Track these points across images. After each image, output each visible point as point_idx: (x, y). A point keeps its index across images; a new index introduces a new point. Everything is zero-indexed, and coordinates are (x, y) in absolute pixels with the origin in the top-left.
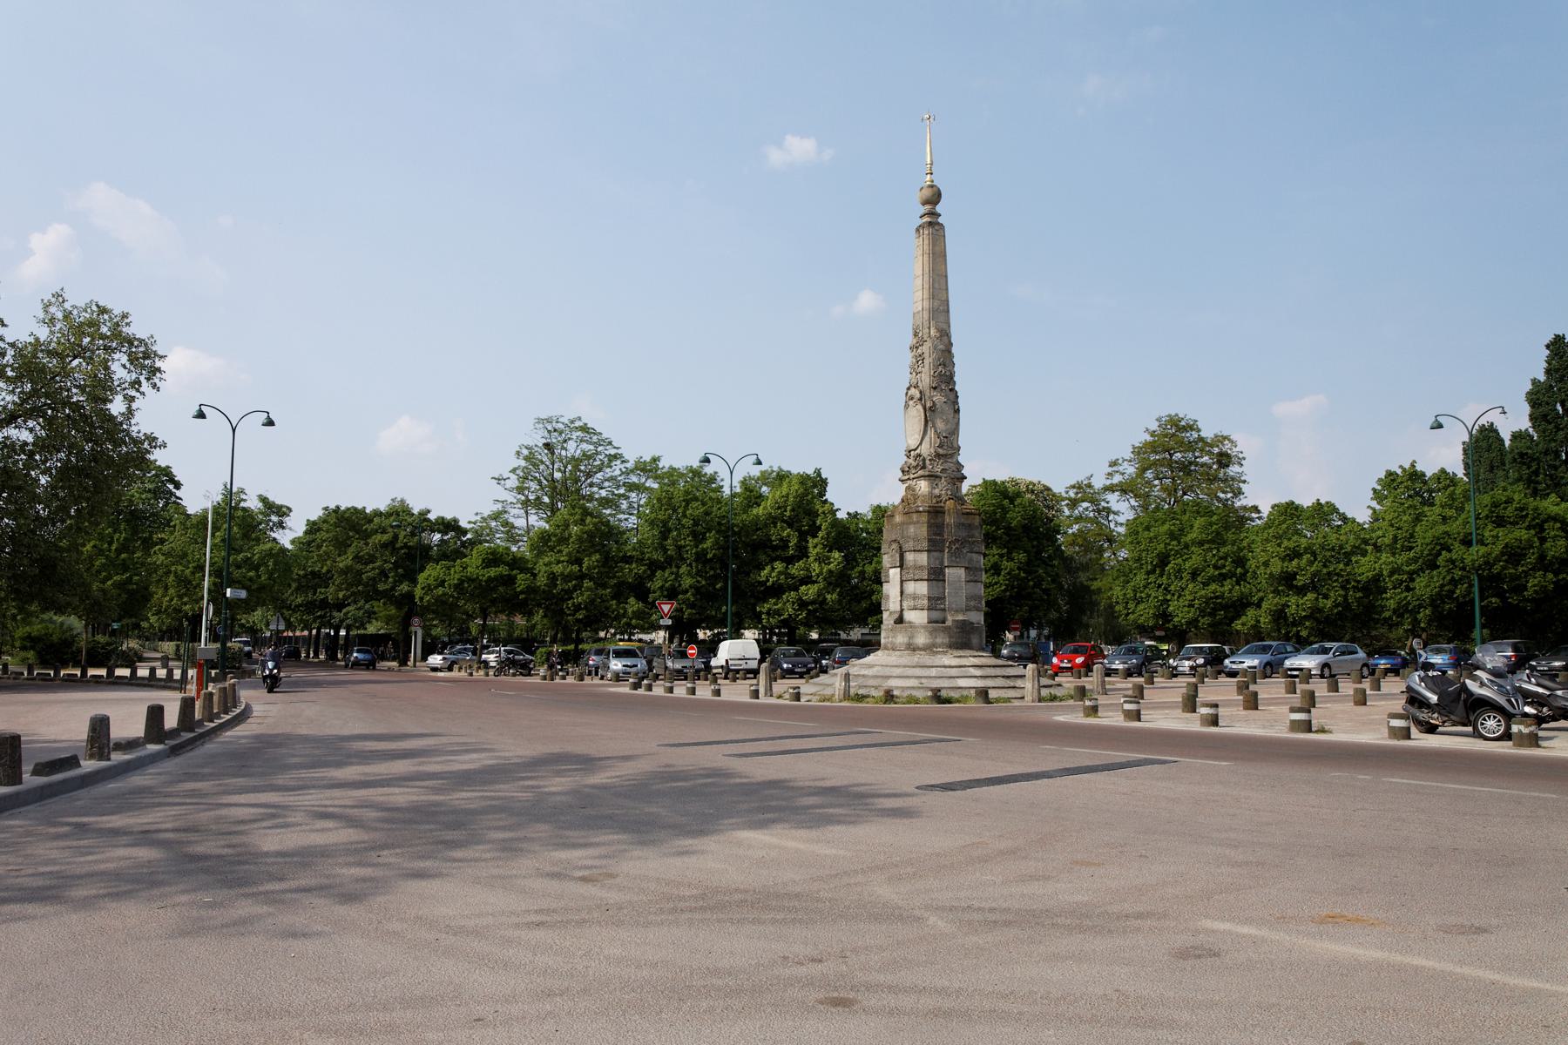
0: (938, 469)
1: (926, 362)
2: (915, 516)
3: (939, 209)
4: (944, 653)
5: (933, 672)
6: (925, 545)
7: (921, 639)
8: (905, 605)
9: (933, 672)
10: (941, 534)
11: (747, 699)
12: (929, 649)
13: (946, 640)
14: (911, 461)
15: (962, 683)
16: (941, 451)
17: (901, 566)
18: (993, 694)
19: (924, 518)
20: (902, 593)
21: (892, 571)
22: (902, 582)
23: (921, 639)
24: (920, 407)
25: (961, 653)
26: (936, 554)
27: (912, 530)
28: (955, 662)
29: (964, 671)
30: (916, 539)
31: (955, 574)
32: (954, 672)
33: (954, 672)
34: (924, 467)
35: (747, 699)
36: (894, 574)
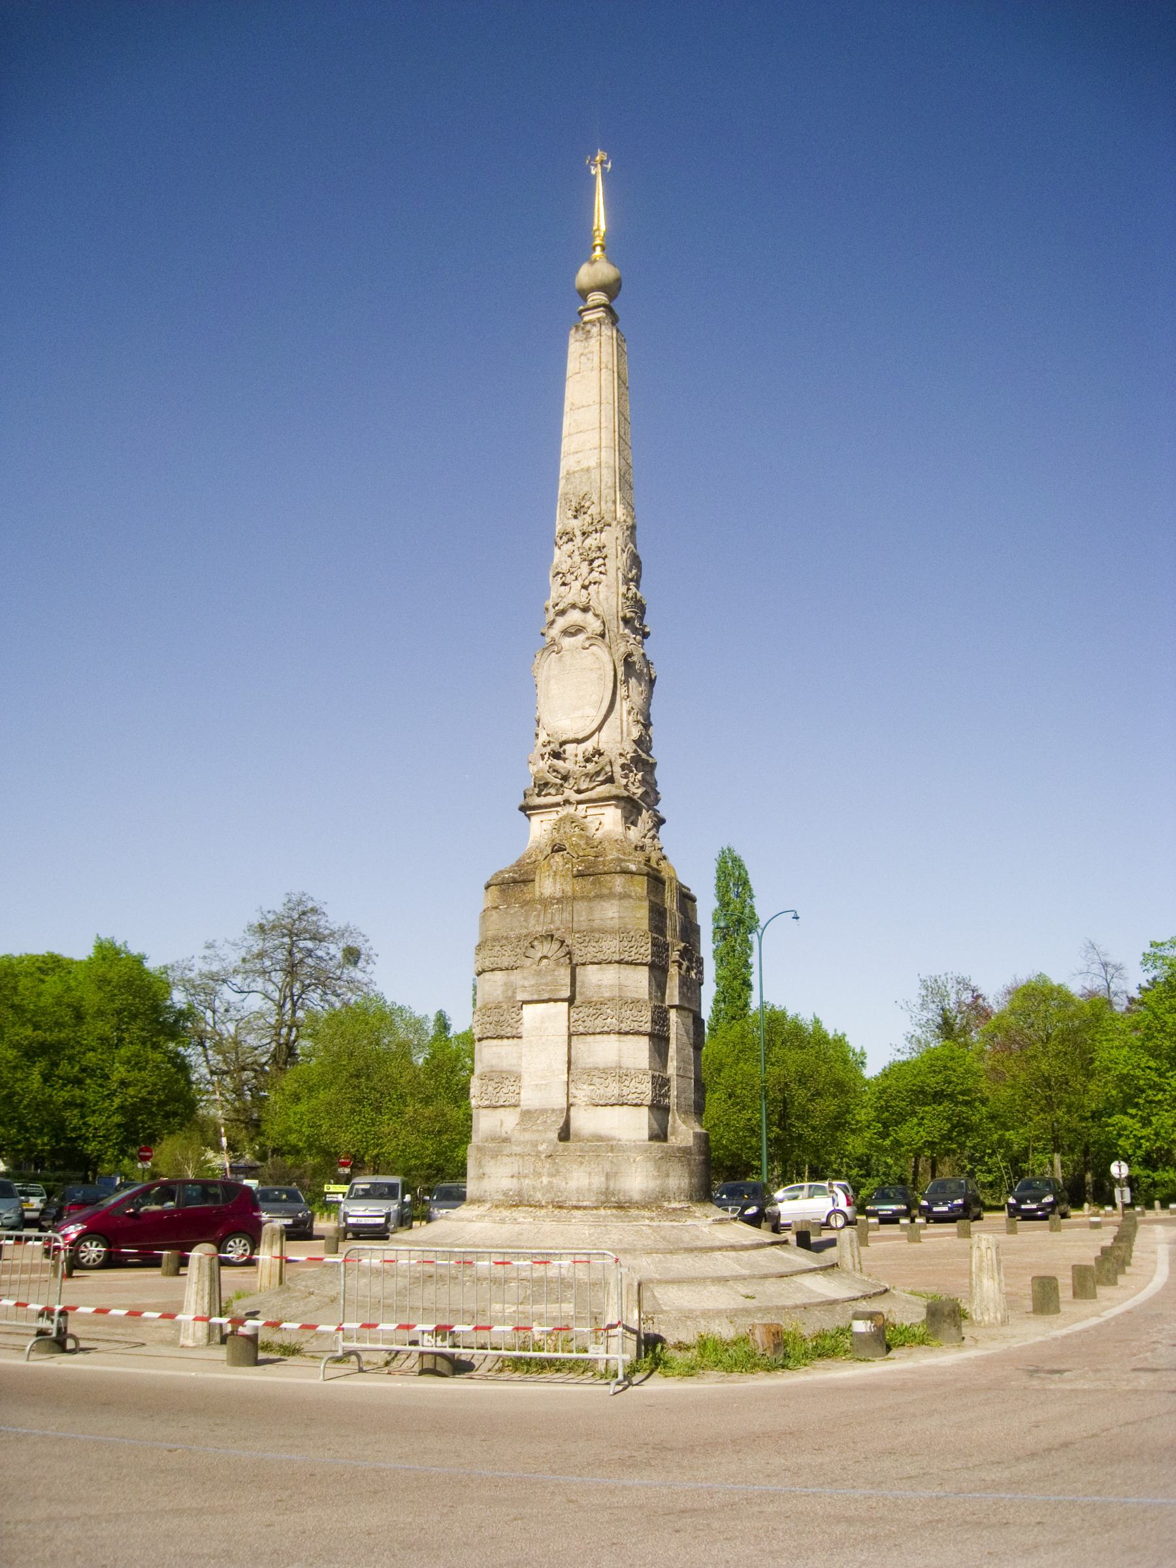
1: (611, 564)
2: (618, 883)
3: (613, 305)
4: (686, 1211)
6: (645, 951)
7: (638, 1180)
8: (582, 1093)
12: (653, 1202)
13: (685, 1183)
17: (571, 1001)
19: (640, 887)
22: (570, 1036)
23: (638, 1180)
26: (657, 973)
27: (610, 913)
30: (623, 932)
34: (610, 780)
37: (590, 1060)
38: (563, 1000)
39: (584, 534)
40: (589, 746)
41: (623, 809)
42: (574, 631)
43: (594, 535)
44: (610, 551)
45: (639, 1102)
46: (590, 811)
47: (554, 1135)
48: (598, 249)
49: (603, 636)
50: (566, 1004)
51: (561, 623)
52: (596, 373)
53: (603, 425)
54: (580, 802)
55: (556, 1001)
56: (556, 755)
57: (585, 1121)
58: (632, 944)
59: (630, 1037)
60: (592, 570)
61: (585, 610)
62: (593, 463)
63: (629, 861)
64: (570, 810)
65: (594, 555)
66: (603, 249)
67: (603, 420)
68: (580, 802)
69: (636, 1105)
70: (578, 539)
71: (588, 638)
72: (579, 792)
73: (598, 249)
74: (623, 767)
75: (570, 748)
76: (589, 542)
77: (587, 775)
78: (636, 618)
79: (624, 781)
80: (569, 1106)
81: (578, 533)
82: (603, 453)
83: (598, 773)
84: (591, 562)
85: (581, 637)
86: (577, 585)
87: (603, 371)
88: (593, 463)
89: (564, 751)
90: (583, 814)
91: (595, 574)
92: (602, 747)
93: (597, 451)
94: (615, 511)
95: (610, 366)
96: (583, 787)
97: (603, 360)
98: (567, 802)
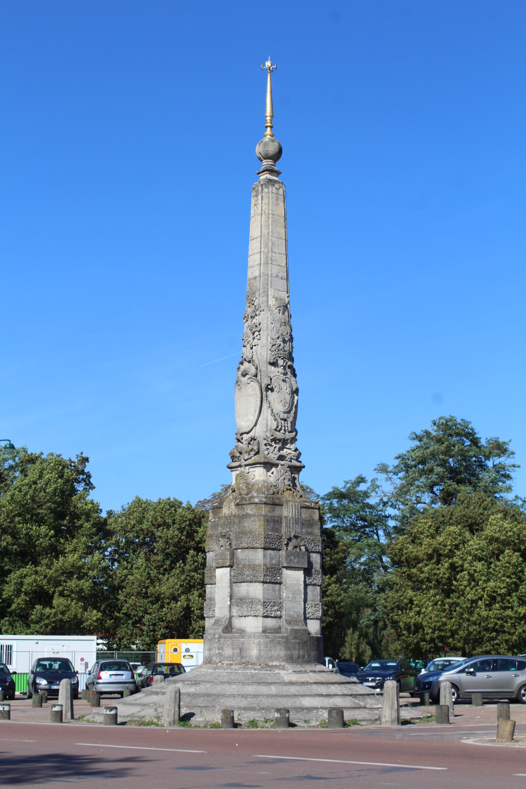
0: (273, 457)
5: (273, 689)
8: (235, 612)
9: (273, 689)
10: (278, 530)
11: (49, 723)
13: (282, 653)
14: (243, 446)
15: (307, 702)
16: (279, 435)
18: (348, 715)
20: (231, 597)
21: (219, 572)
24: (255, 385)
25: (298, 668)
28: (294, 678)
29: (317, 691)
31: (294, 578)
32: (293, 689)
33: (293, 689)
35: (49, 723)
36: (222, 575)
37: (238, 595)
38: (228, 567)
39: (251, 317)
40: (251, 434)
41: (264, 467)
42: (244, 375)
43: (256, 317)
44: (263, 326)
45: (256, 614)
46: (251, 470)
47: (220, 630)
48: (269, 129)
49: (256, 376)
50: (229, 568)
51: (242, 368)
52: (259, 217)
53: (262, 250)
54: (246, 465)
55: (226, 567)
56: (239, 441)
57: (238, 623)
58: (253, 539)
59: (253, 584)
60: (254, 338)
61: (249, 362)
62: (257, 274)
63: (256, 497)
64: (243, 469)
65: (254, 330)
66: (271, 127)
67: (262, 247)
68: (246, 465)
69: (255, 616)
70: (249, 320)
71: (249, 378)
72: (246, 460)
73: (269, 129)
74: (266, 445)
75: (245, 436)
76: (254, 321)
77: (246, 452)
78: (286, 359)
79: (266, 452)
80: (231, 617)
81: (249, 317)
82: (262, 267)
83: (251, 450)
84: (254, 334)
85: (248, 376)
86: (248, 346)
87: (263, 215)
88: (257, 274)
89: (242, 439)
90: (247, 471)
91: (256, 340)
92: (257, 435)
93: (259, 266)
94: (267, 301)
95: (267, 211)
96: (246, 458)
97: (263, 208)
98: (240, 466)
